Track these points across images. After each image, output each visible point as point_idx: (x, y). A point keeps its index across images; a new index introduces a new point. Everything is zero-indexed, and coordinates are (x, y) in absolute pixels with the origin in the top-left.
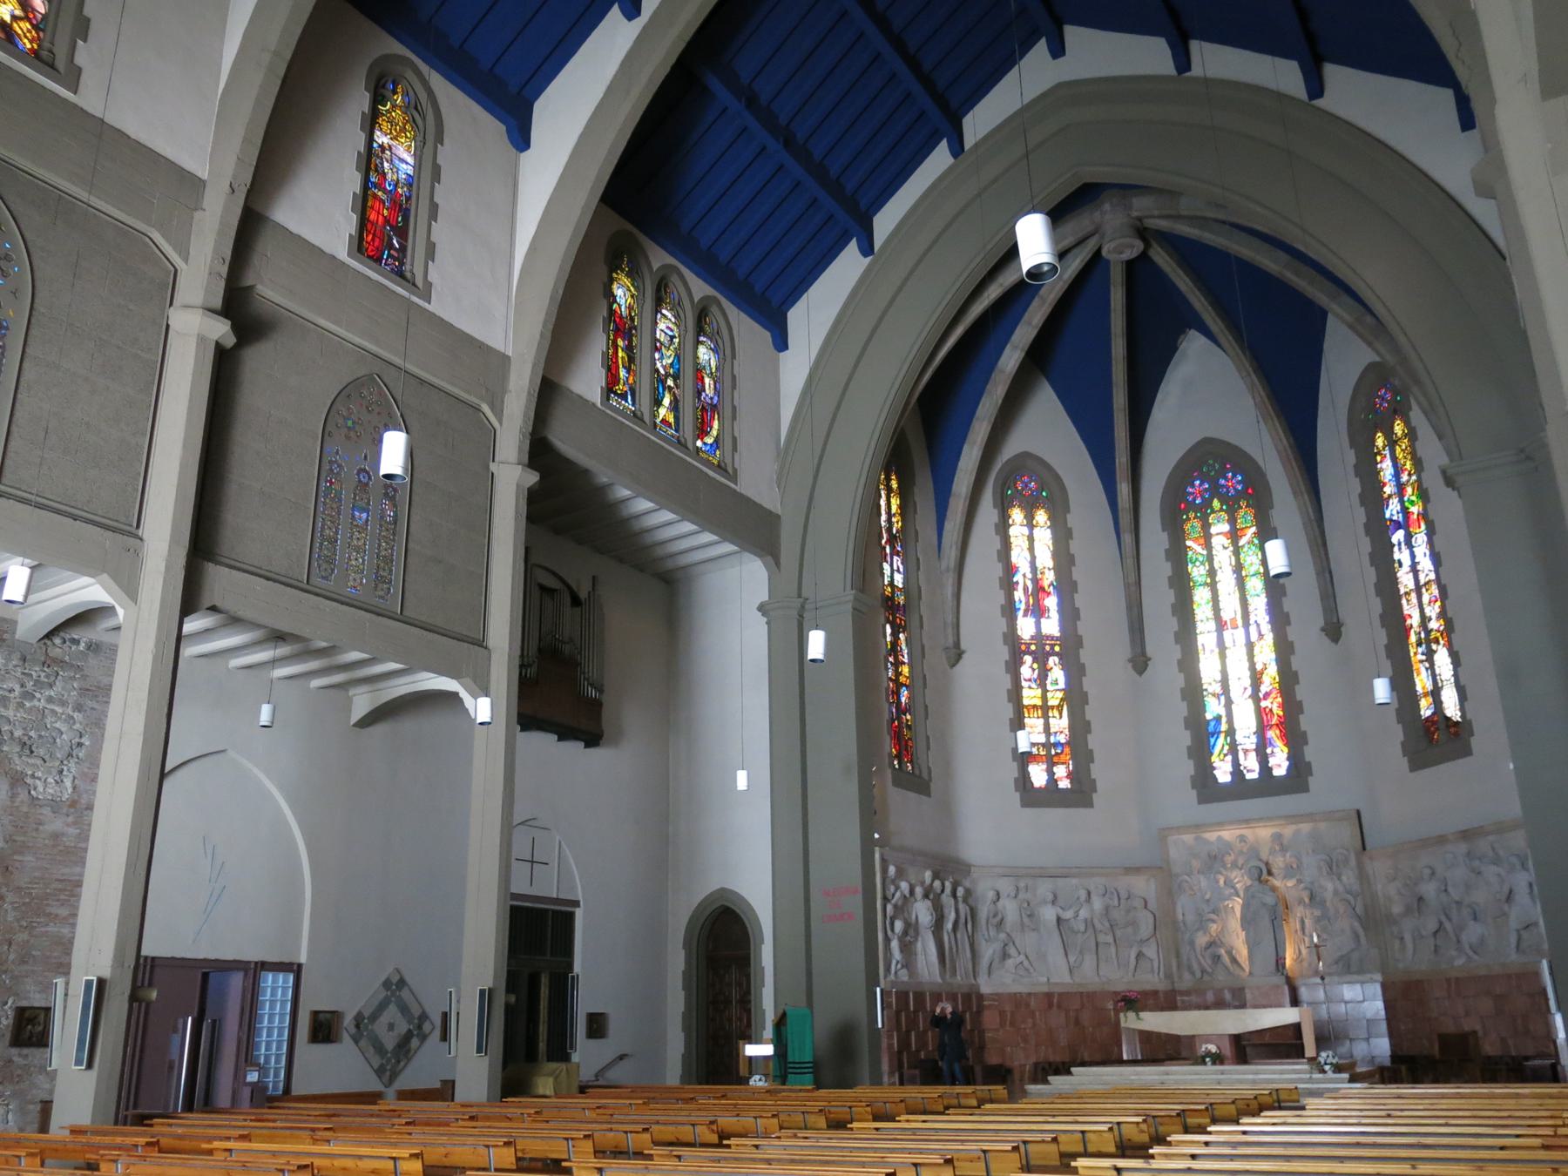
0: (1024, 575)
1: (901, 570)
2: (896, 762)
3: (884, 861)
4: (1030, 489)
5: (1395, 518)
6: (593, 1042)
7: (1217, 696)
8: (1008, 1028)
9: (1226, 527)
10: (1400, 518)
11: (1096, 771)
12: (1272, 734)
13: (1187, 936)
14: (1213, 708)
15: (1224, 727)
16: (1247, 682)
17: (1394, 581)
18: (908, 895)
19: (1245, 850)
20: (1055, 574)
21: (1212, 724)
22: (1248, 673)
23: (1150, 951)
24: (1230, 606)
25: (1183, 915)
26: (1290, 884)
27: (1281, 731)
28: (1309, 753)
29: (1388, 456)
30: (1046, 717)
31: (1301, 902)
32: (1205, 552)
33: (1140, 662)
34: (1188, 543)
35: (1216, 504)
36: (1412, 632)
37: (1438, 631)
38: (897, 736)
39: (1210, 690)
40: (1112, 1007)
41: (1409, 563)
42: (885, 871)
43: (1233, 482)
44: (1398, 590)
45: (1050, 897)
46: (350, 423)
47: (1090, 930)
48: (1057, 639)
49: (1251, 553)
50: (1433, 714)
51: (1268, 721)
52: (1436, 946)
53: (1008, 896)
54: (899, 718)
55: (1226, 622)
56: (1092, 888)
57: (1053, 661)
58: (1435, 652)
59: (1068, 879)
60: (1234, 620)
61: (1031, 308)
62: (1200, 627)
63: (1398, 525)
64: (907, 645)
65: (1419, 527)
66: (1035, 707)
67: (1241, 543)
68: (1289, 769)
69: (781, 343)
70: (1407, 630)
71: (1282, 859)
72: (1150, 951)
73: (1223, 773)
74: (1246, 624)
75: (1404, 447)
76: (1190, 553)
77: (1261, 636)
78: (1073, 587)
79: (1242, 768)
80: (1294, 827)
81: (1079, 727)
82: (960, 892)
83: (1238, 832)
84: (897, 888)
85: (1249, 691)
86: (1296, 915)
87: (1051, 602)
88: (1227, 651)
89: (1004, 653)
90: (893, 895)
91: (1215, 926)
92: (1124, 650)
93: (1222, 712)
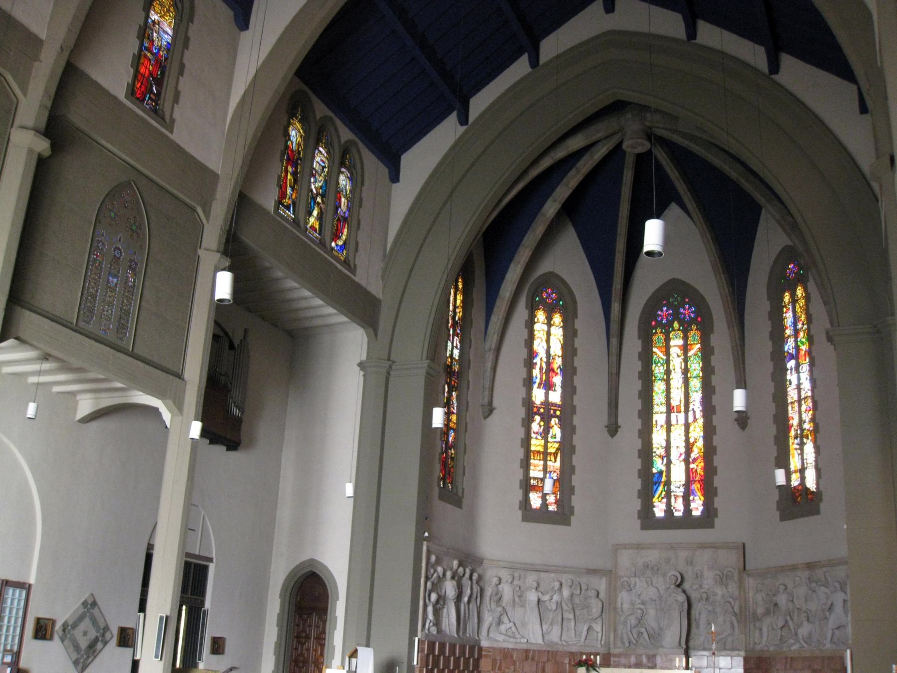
0: (541, 359)
1: (459, 347)
2: (442, 483)
3: (429, 552)
4: (552, 299)
5: (791, 351)
6: (215, 657)
7: (662, 458)
8: (496, 671)
9: (680, 342)
10: (793, 352)
11: (576, 501)
12: (696, 487)
13: (622, 619)
14: (658, 465)
15: (664, 479)
16: (683, 450)
17: (785, 393)
18: (441, 576)
20: (562, 361)
21: (656, 476)
22: (684, 444)
23: (597, 627)
24: (677, 397)
25: (622, 604)
27: (701, 485)
28: (718, 502)
29: (791, 309)
30: (545, 460)
32: (665, 357)
33: (613, 429)
34: (655, 350)
35: (676, 325)
36: (793, 429)
37: (809, 430)
38: (444, 464)
39: (658, 452)
40: (568, 662)
41: (796, 383)
42: (428, 559)
43: (688, 311)
44: (787, 400)
45: (535, 585)
46: (113, 214)
47: (559, 610)
48: (559, 406)
49: (695, 362)
50: (799, 485)
51: (693, 478)
52: (781, 635)
53: (507, 581)
54: (446, 452)
55: (673, 407)
56: (564, 582)
57: (554, 421)
58: (805, 444)
59: (549, 574)
60: (678, 406)
61: (569, 175)
62: (656, 409)
63: (792, 357)
64: (457, 400)
65: (805, 360)
66: (538, 452)
67: (690, 353)
68: (703, 512)
69: (395, 177)
70: (789, 427)
72: (597, 627)
73: (659, 510)
74: (687, 411)
75: (801, 305)
76: (655, 356)
77: (695, 419)
78: (574, 371)
81: (567, 470)
82: (475, 577)
84: (435, 571)
85: (683, 457)
87: (557, 380)
88: (672, 427)
89: (522, 412)
90: (432, 575)
92: (604, 419)
93: (664, 468)
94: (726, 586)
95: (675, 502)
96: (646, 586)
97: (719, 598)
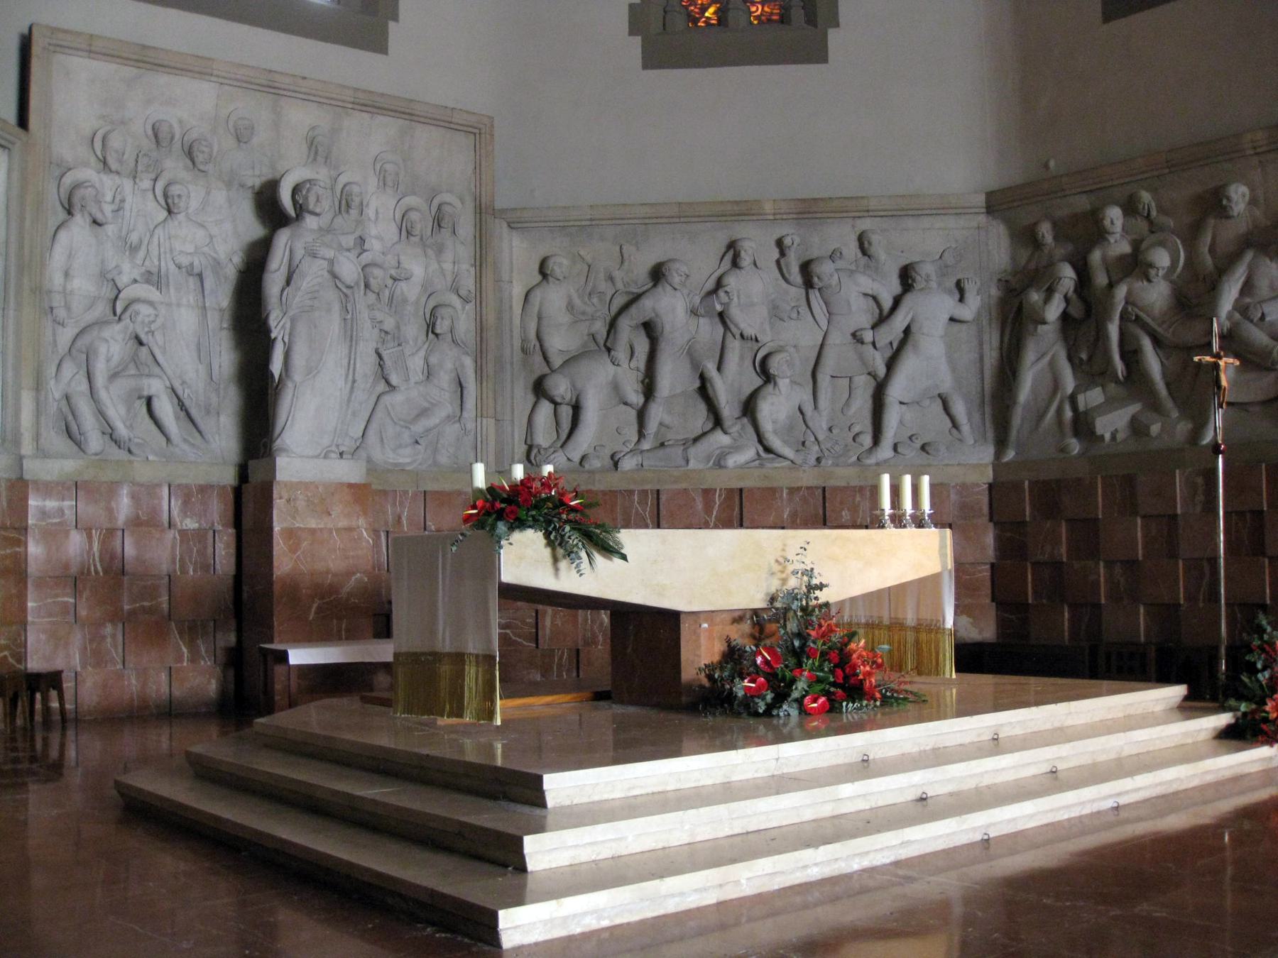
13: (66, 335)
25: (67, 274)
94: (440, 250)
96: (165, 213)
97: (411, 291)
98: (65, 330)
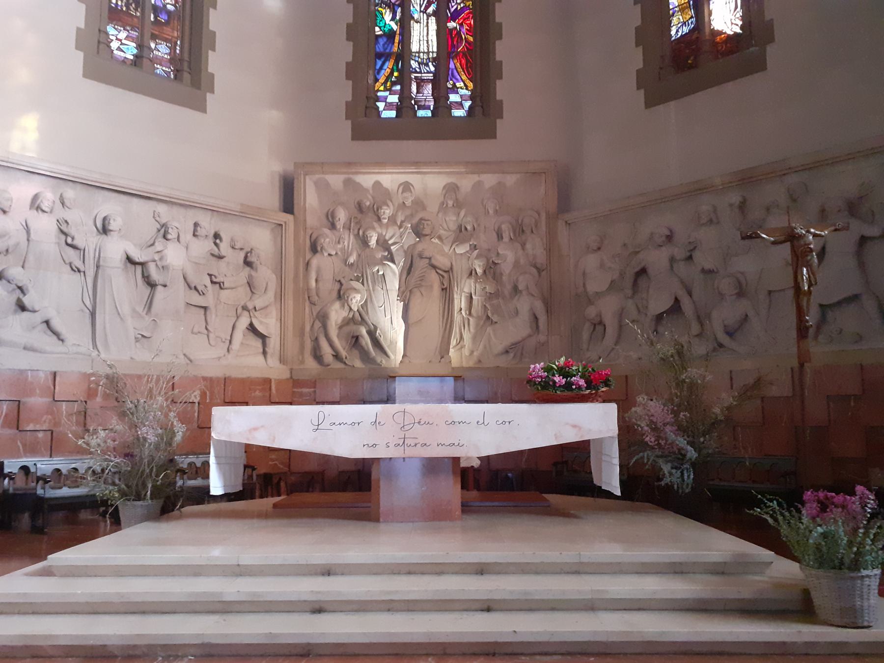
19: (408, 203)
21: (382, 41)
25: (317, 281)
26: (461, 250)
31: (471, 273)
71: (454, 218)
79: (413, 102)
80: (475, 178)
83: (403, 178)
86: (462, 291)
91: (358, 297)
94: (523, 246)
95: (418, 92)
98: (316, 307)
